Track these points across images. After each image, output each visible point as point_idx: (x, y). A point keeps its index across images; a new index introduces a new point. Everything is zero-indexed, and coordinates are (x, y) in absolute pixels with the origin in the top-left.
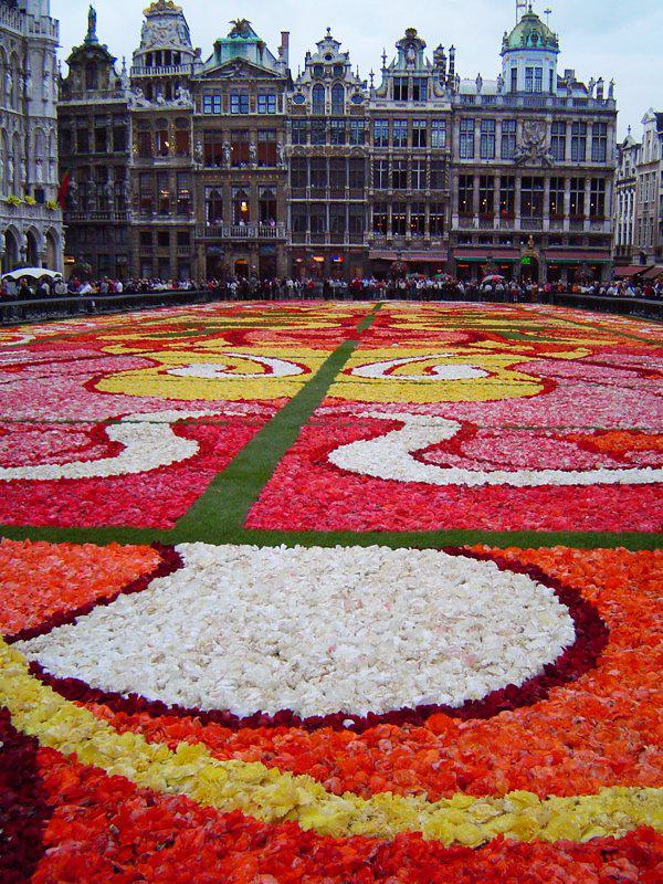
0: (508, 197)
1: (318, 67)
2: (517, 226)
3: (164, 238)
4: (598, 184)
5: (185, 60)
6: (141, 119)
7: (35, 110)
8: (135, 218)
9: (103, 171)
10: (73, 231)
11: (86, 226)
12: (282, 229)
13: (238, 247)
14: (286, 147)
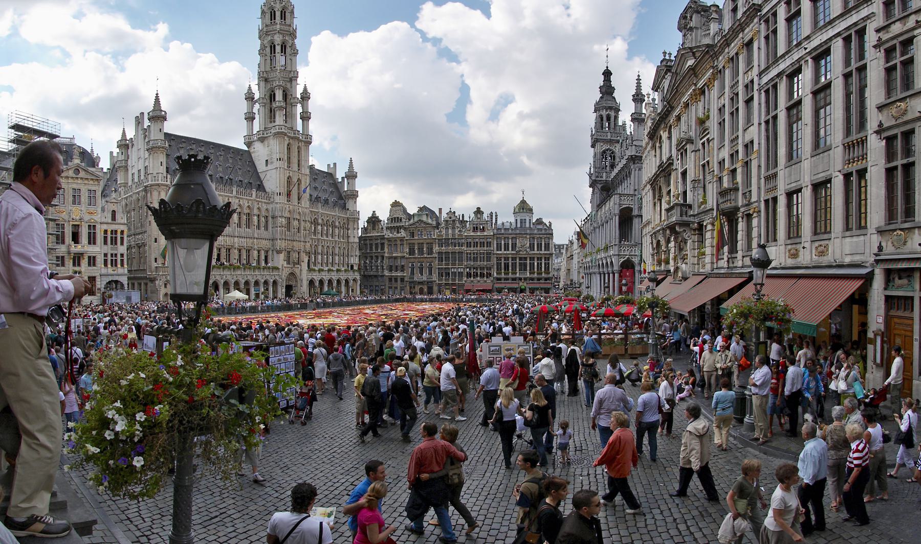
0: (514, 265)
1: (447, 221)
2: (518, 275)
3: (396, 280)
4: (547, 259)
5: (403, 220)
6: (389, 240)
7: (351, 240)
8: (386, 273)
9: (377, 257)
10: (365, 277)
11: (370, 276)
12: (435, 277)
13: (420, 283)
14: (436, 248)
